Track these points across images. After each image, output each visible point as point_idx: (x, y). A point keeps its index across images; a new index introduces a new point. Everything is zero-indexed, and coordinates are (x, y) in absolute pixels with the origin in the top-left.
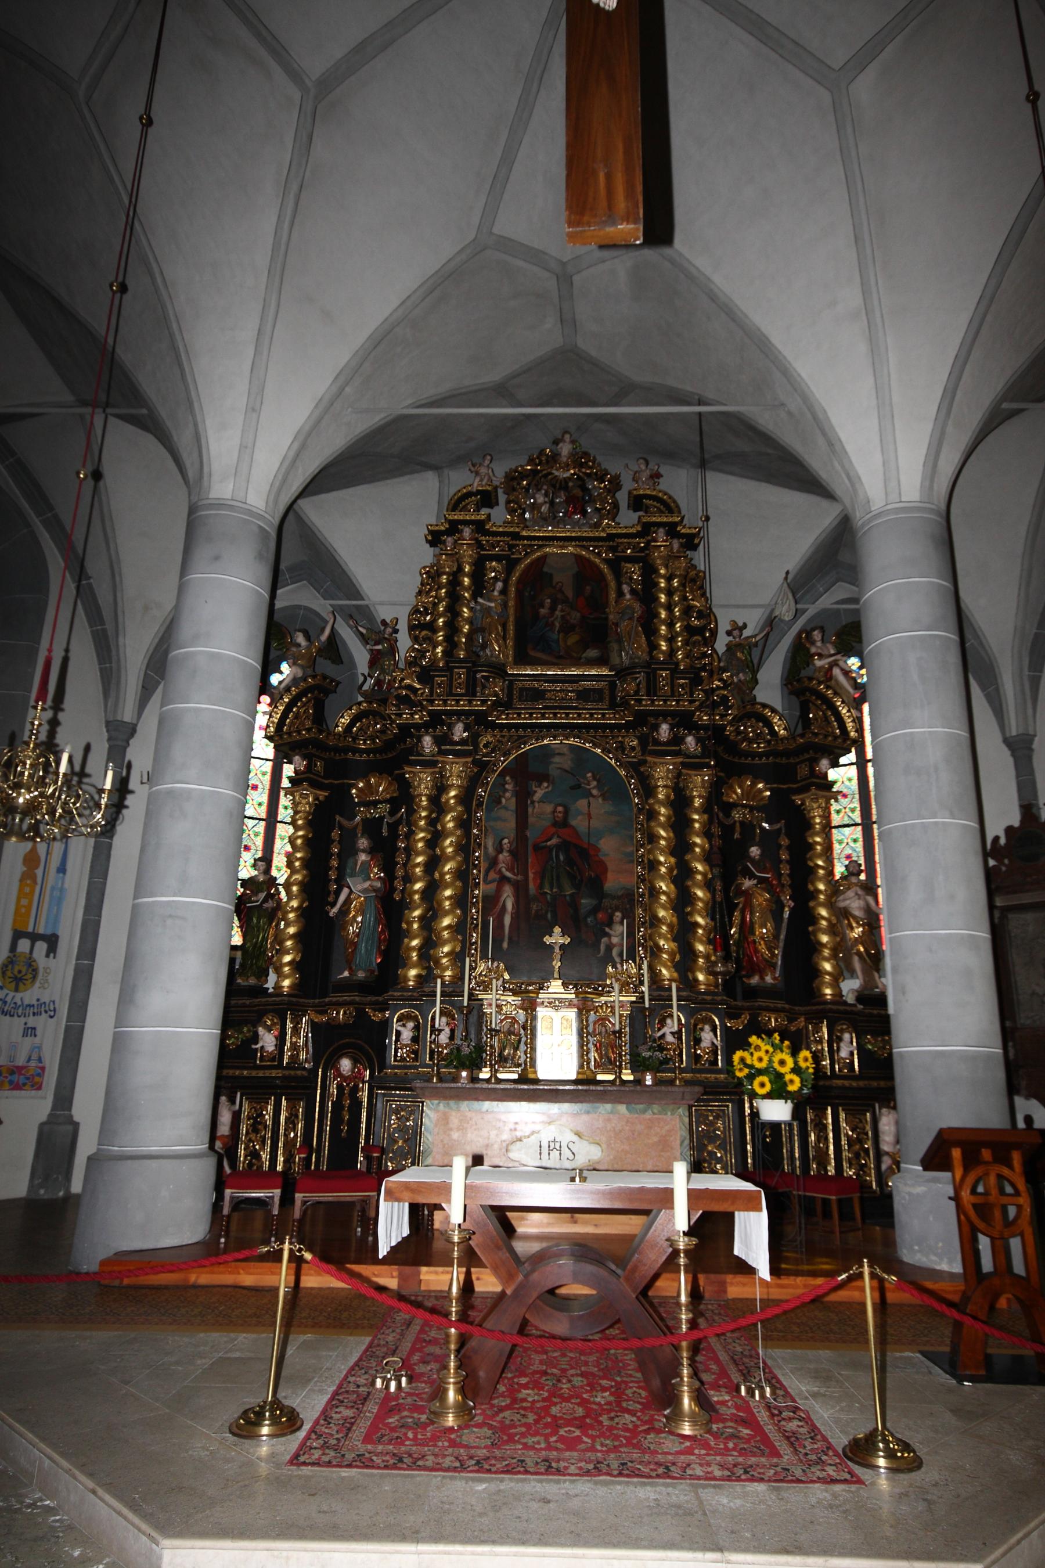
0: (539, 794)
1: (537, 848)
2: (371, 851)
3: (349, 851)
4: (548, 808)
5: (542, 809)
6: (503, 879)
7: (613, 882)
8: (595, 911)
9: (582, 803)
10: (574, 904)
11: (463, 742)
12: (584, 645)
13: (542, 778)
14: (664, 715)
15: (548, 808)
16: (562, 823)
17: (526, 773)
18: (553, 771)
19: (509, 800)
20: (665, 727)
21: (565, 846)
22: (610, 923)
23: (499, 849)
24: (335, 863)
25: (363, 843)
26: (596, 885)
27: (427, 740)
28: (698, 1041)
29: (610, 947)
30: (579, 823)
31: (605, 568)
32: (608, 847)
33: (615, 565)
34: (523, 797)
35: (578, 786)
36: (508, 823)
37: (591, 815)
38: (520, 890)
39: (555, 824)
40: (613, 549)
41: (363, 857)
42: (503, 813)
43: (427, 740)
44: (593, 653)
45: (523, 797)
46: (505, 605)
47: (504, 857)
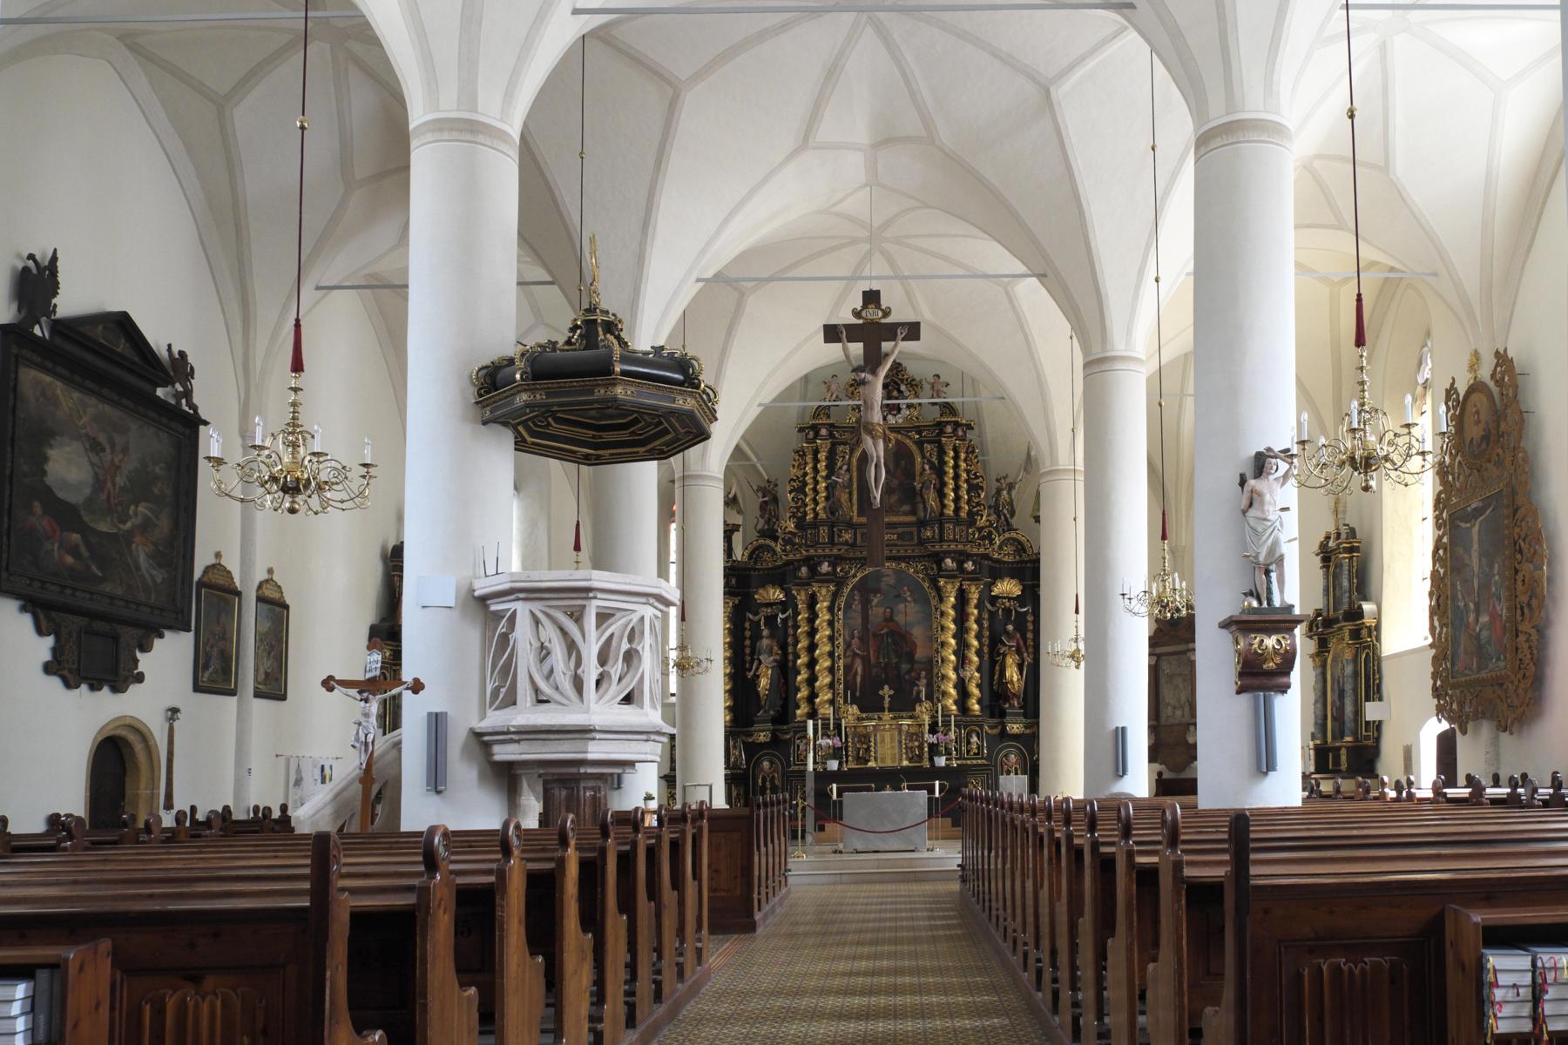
0: (875, 601)
1: (875, 635)
2: (771, 636)
3: (757, 636)
4: (881, 610)
5: (877, 612)
6: (855, 655)
7: (920, 654)
8: (909, 672)
9: (901, 606)
10: (897, 668)
11: (828, 574)
12: (901, 502)
13: (877, 591)
14: (948, 553)
15: (881, 610)
16: (889, 619)
17: (866, 589)
18: (883, 586)
19: (857, 606)
20: (949, 561)
21: (891, 633)
22: (919, 678)
23: (852, 637)
24: (748, 642)
25: (765, 633)
26: (910, 657)
27: (804, 570)
28: (969, 743)
29: (919, 692)
30: (900, 619)
31: (914, 448)
32: (917, 633)
33: (920, 444)
34: (866, 604)
35: (898, 596)
36: (857, 620)
37: (908, 613)
38: (866, 660)
39: (886, 620)
40: (919, 433)
41: (765, 642)
42: (853, 615)
43: (804, 570)
44: (906, 508)
45: (866, 604)
46: (851, 479)
47: (855, 641)
